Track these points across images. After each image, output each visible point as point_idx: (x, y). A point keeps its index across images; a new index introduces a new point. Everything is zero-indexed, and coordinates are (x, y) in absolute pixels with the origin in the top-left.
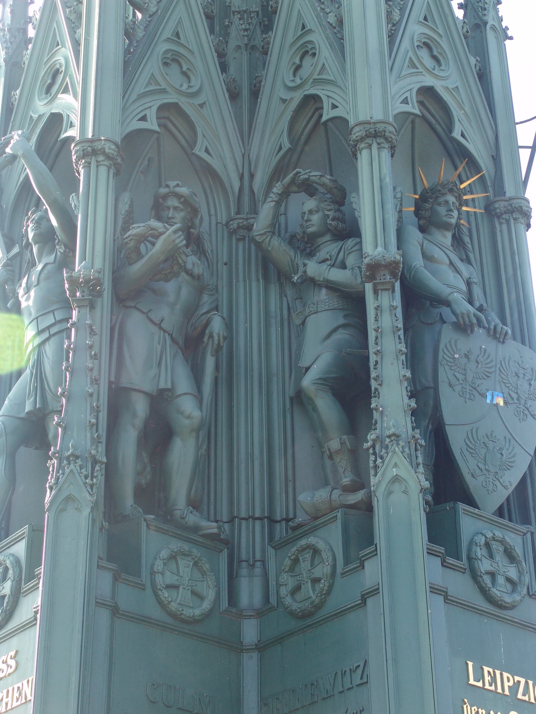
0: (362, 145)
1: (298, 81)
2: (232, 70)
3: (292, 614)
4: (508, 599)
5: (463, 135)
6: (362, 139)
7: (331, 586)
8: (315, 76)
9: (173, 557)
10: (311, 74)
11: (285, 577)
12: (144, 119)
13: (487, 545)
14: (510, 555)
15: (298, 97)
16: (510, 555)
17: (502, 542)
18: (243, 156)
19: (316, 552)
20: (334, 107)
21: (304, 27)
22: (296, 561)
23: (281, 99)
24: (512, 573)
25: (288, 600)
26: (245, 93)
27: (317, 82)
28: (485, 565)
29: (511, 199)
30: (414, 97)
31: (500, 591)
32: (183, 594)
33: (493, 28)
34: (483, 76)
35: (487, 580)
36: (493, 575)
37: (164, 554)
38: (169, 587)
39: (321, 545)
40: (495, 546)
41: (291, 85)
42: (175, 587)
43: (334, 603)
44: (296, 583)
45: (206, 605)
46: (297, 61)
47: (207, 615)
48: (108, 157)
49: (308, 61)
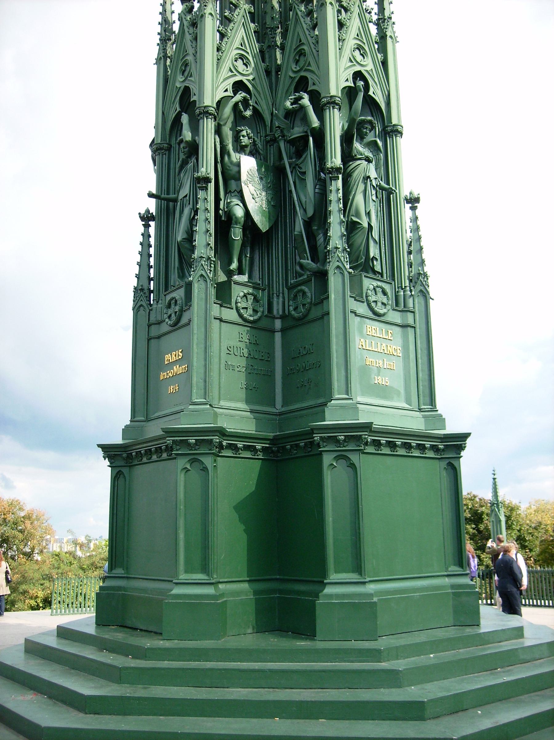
0: (325, 108)
1: (298, 68)
2: (267, 60)
3: (294, 318)
4: (382, 312)
5: (374, 93)
6: (325, 105)
7: (310, 308)
8: (306, 68)
9: (245, 296)
10: (303, 66)
11: (291, 302)
12: (226, 90)
13: (374, 289)
14: (384, 293)
15: (298, 76)
16: (384, 293)
17: (381, 287)
18: (273, 105)
19: (304, 293)
20: (314, 84)
21: (300, 41)
22: (296, 296)
23: (290, 76)
24: (385, 301)
25: (293, 312)
26: (273, 73)
27: (306, 70)
28: (372, 298)
29: (394, 125)
30: (351, 79)
31: (380, 309)
32: (250, 311)
33: (391, 37)
34: (384, 63)
35: (373, 305)
36: (376, 302)
37: (242, 294)
38: (243, 308)
39: (306, 290)
40: (378, 289)
41: (295, 70)
42: (246, 308)
43: (312, 316)
44: (296, 306)
45: (259, 314)
46: (297, 58)
47: (260, 319)
48: (210, 114)
49: (302, 59)
